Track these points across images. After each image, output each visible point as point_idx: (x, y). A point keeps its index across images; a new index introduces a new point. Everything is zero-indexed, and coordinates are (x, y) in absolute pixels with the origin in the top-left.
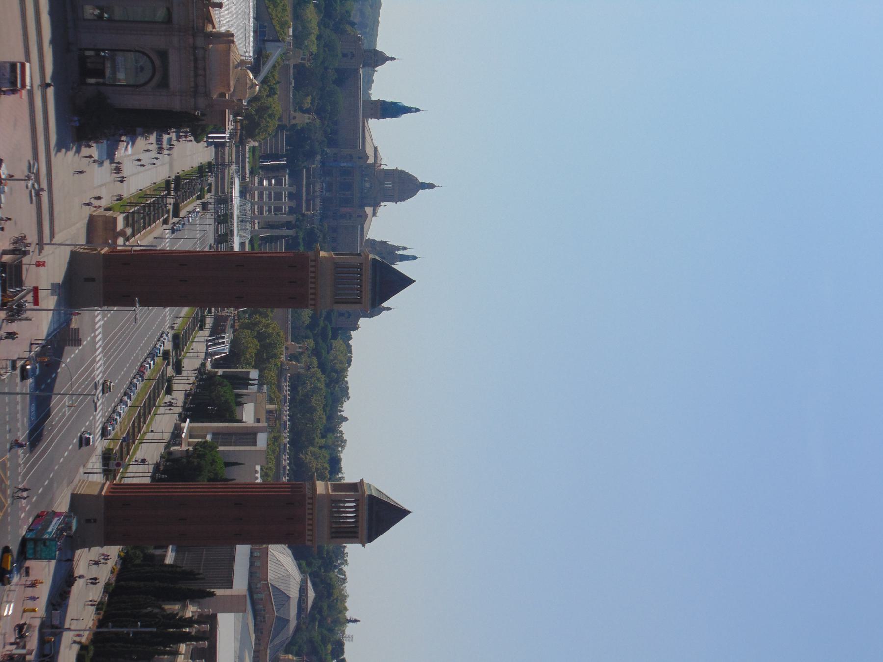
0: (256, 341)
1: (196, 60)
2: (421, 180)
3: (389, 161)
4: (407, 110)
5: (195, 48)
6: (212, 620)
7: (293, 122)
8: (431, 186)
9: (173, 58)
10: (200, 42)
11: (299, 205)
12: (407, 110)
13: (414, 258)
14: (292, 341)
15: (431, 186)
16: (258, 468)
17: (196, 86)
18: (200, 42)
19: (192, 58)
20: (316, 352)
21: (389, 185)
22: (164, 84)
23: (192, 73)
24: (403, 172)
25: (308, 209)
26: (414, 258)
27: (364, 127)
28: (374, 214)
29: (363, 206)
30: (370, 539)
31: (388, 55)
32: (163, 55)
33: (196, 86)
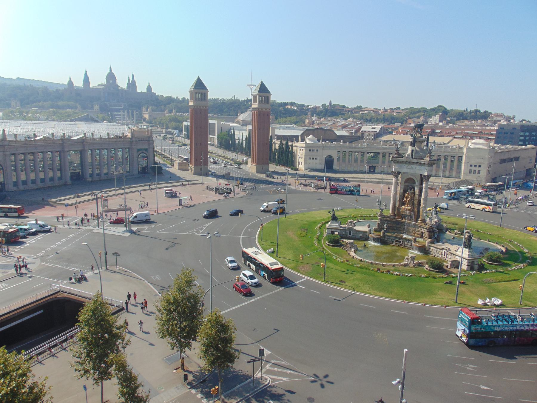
0: (172, 123)
1: (139, 141)
2: (109, 71)
3: (104, 82)
4: (86, 74)
5: (136, 141)
6: (279, 137)
7: (99, 110)
8: (111, 68)
9: (139, 147)
10: (134, 140)
11: (121, 109)
12: (86, 74)
13: (133, 75)
14: (165, 112)
15: (111, 68)
16: (222, 123)
17: (146, 141)
18: (134, 140)
19: (139, 142)
20: (165, 105)
21: (111, 81)
22: (146, 150)
23: (143, 142)
24: (107, 77)
25: (122, 107)
26: (133, 75)
27: (92, 88)
28: (120, 86)
29: (118, 90)
30: (270, 93)
31: (69, 79)
32: (139, 150)
33: (146, 141)
